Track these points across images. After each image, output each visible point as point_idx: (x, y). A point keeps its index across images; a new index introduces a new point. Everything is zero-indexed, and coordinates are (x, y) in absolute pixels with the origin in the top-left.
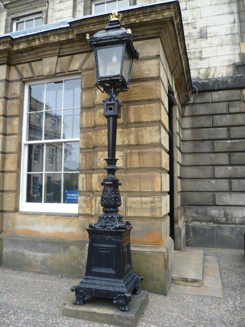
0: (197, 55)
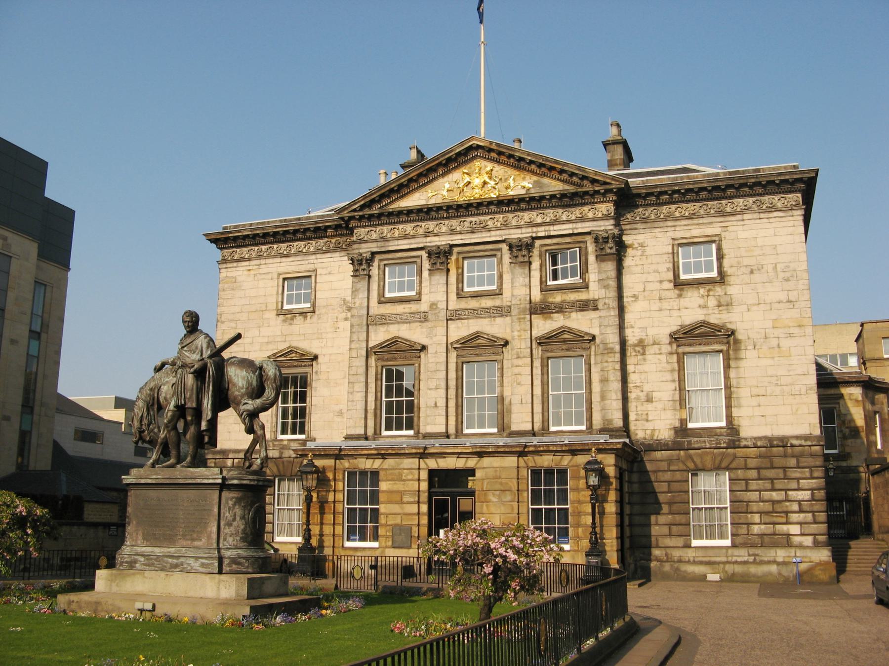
0: (644, 417)
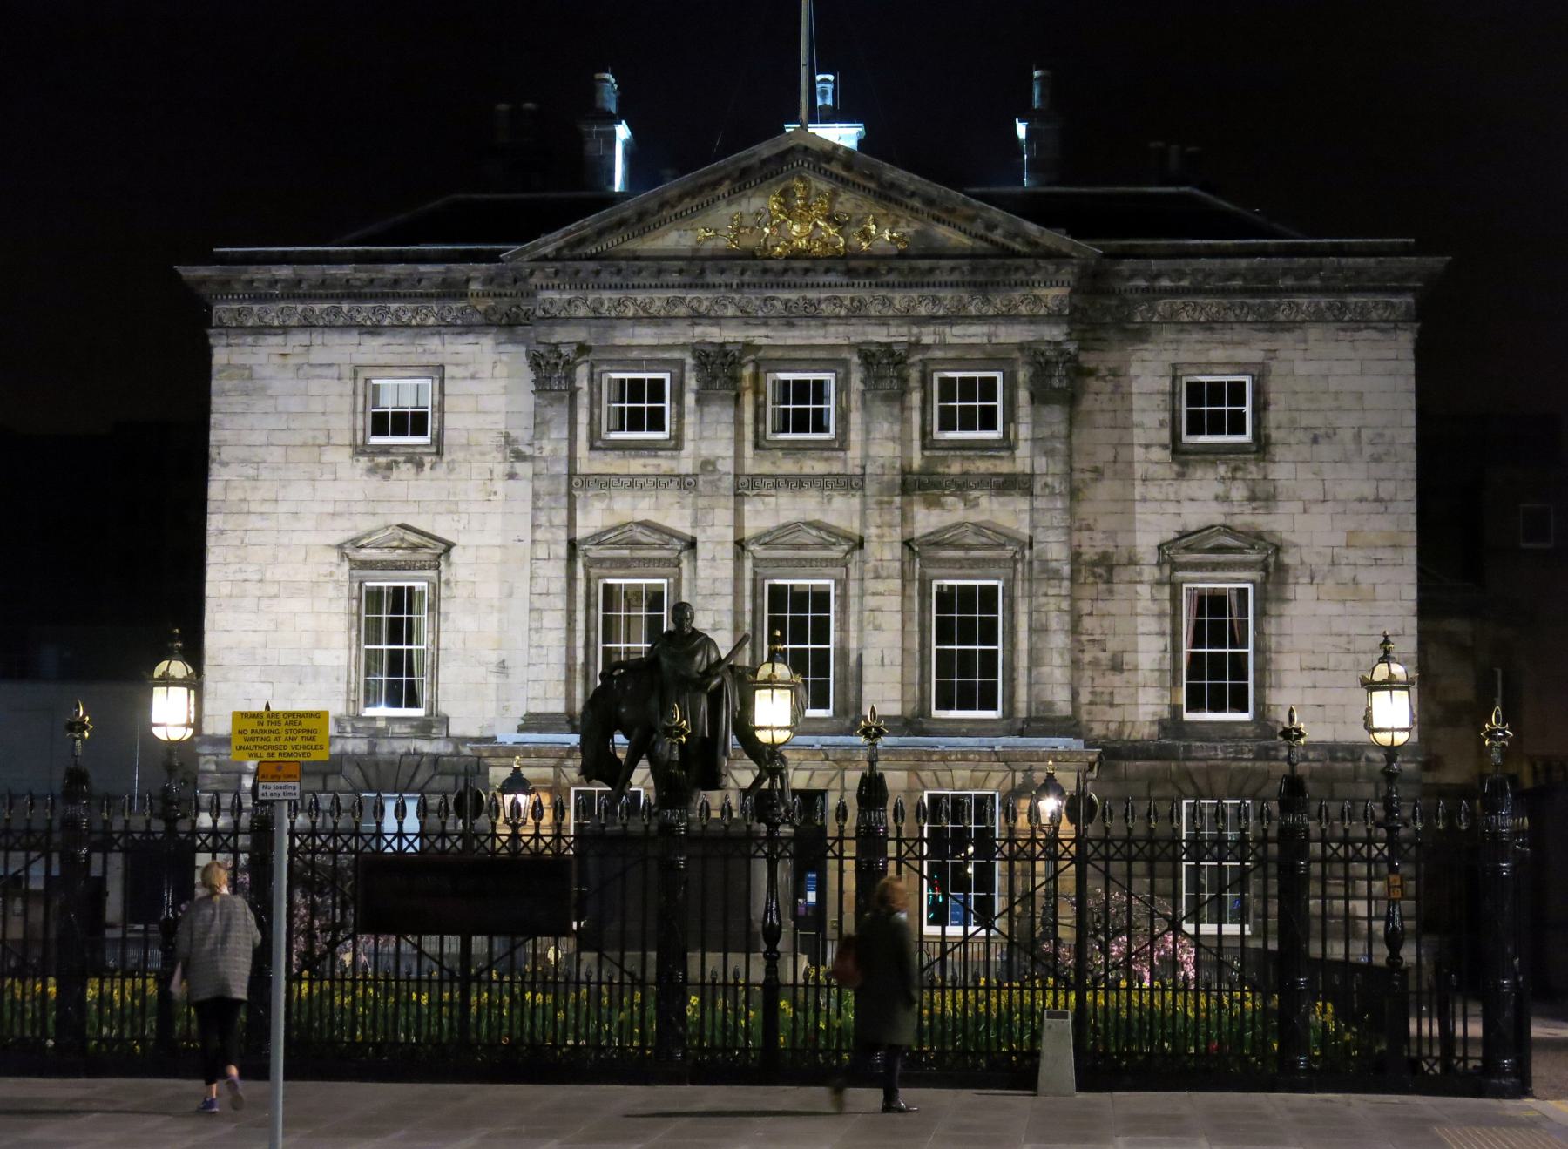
0: (1106, 698)
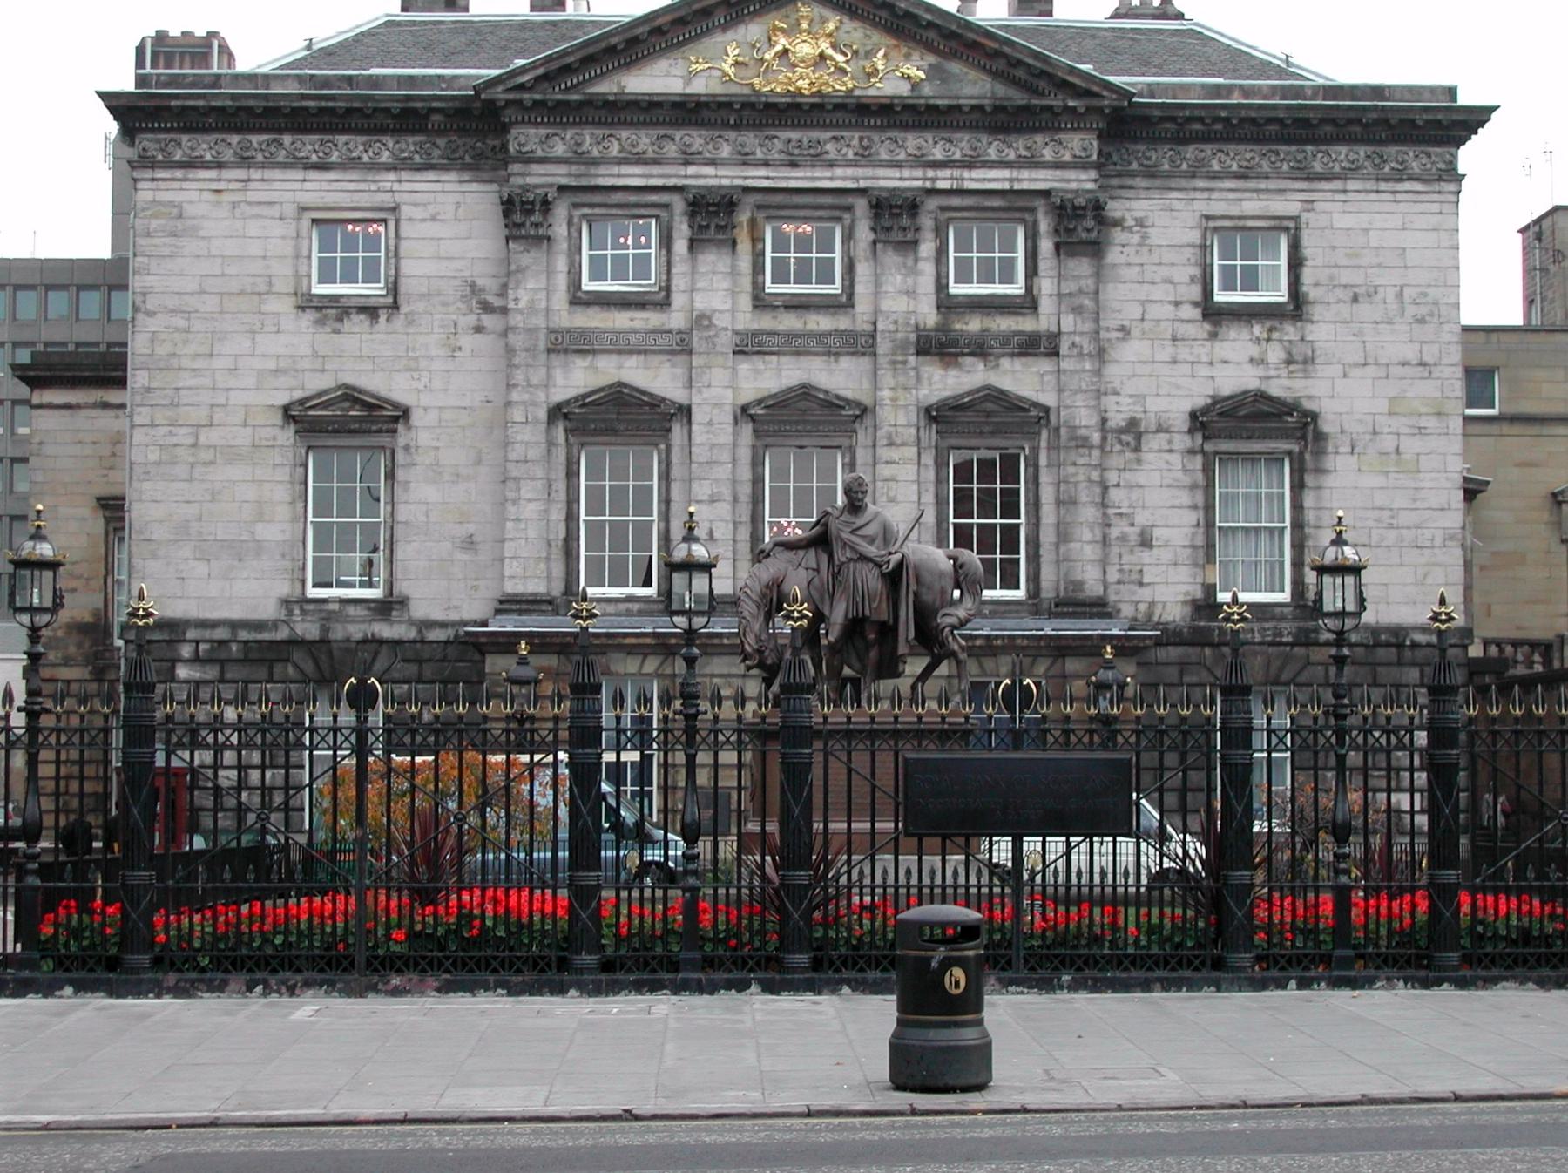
0: (1135, 576)
